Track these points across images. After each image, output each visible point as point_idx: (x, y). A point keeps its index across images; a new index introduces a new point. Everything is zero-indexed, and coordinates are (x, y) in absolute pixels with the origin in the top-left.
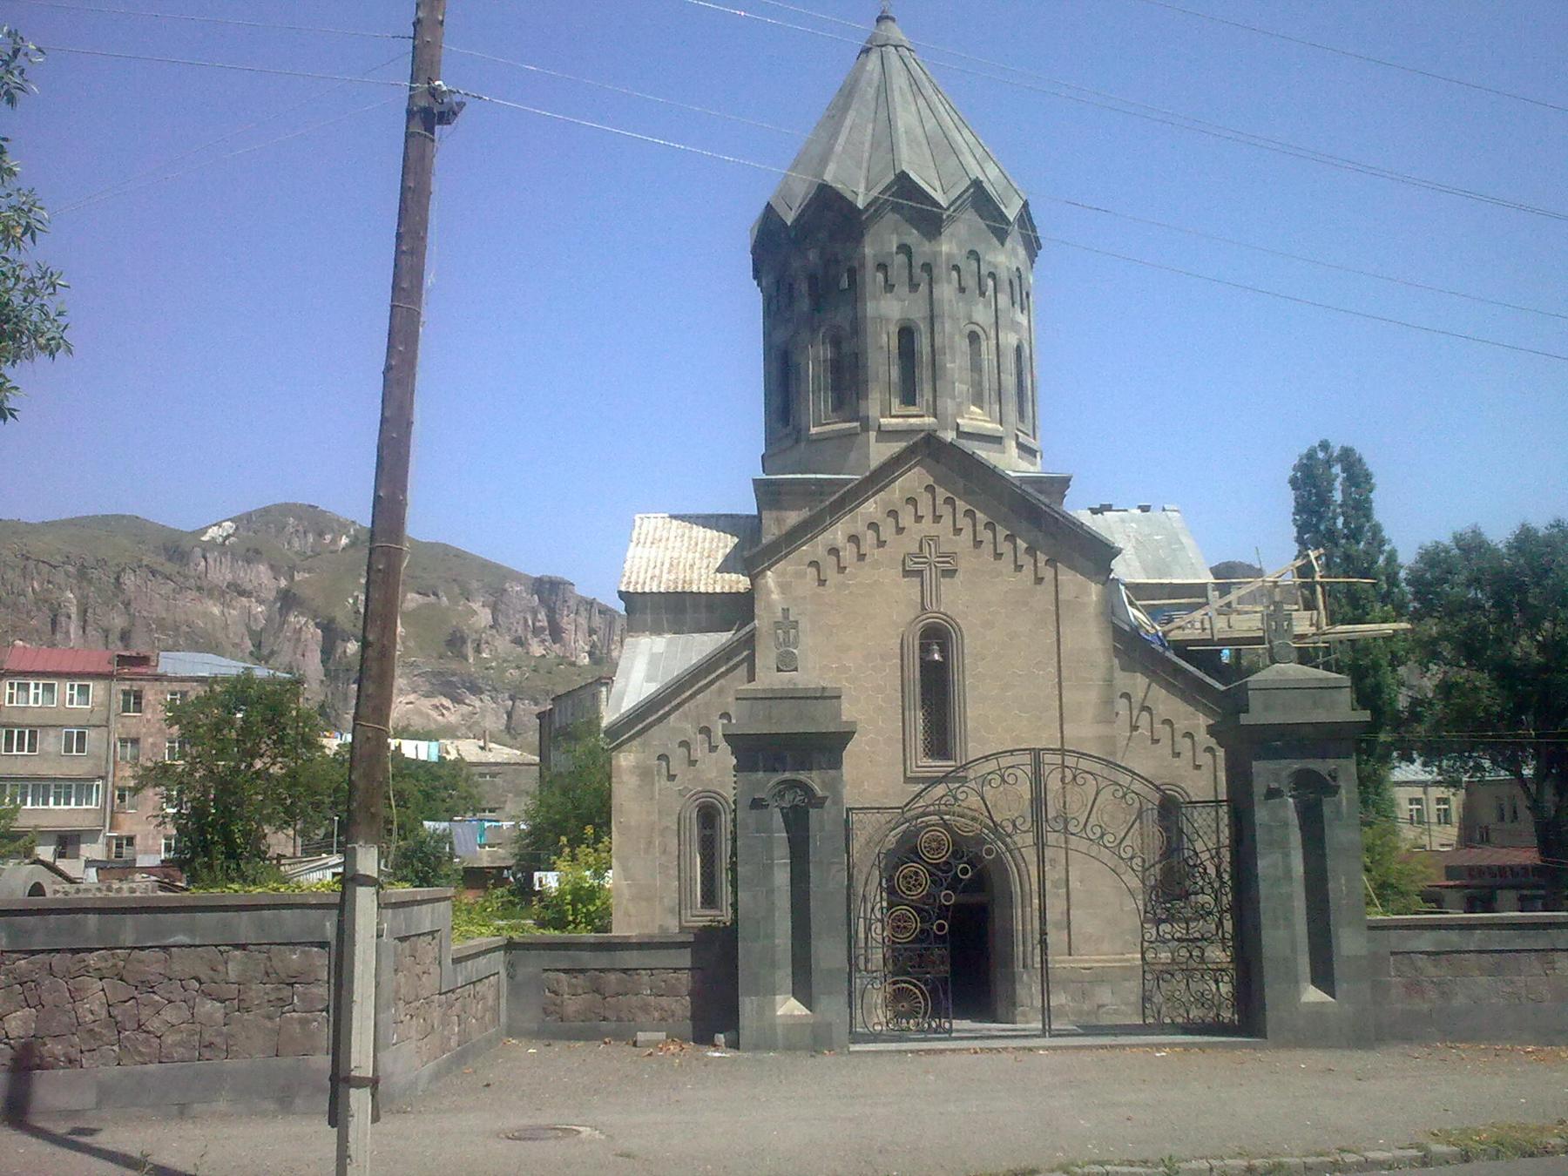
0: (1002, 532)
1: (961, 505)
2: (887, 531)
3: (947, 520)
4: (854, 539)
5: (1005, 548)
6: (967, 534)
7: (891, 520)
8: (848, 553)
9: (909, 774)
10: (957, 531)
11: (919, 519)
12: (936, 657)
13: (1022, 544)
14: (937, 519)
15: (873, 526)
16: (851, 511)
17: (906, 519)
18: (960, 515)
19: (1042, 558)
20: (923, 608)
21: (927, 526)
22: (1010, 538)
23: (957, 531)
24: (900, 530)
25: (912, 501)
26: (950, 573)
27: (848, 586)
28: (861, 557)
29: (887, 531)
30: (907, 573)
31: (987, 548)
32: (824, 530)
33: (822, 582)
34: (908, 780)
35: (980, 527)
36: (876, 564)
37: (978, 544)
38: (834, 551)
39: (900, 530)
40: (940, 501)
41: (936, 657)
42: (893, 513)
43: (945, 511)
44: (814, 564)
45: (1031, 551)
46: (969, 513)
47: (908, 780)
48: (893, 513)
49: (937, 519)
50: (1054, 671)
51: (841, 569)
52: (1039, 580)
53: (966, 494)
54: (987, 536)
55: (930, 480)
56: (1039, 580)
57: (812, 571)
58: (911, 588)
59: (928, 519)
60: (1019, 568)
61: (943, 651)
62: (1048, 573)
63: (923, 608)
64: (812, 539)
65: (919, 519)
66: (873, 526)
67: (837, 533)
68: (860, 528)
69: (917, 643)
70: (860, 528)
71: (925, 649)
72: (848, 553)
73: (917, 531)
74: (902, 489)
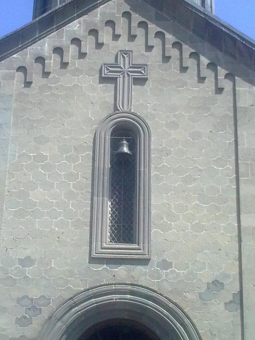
0: (187, 50)
1: (153, 28)
2: (88, 45)
3: (140, 41)
4: (58, 50)
5: (190, 63)
6: (157, 51)
7: (92, 38)
8: (53, 62)
9: (94, 255)
10: (149, 48)
11: (116, 37)
12: (126, 149)
13: (204, 61)
14: (132, 38)
15: (76, 41)
16: (58, 28)
17: (105, 36)
18: (151, 35)
19: (222, 72)
20: (116, 109)
21: (123, 43)
22: (195, 55)
23: (149, 48)
24: (99, 45)
25: (110, 23)
26: (141, 81)
27: (50, 88)
28: (64, 65)
29: (88, 45)
30: (103, 80)
31: (174, 63)
32: (34, 42)
33: (28, 84)
34: (93, 260)
35: (168, 46)
36: (76, 72)
37: (166, 59)
38: (40, 60)
39: (99, 45)
40: (134, 24)
41: (126, 149)
42: (94, 32)
43: (140, 32)
44: (22, 69)
45: (212, 66)
46: (159, 35)
47: (93, 260)
48: (94, 32)
49: (132, 38)
50: (231, 167)
51: (46, 74)
52: (219, 90)
53: (158, 19)
54: (174, 53)
55: (127, 8)
56: (219, 90)
57: (21, 74)
58: (106, 93)
59: (124, 38)
60: (201, 80)
61: (132, 146)
62: (227, 85)
63: (116, 109)
64: (22, 49)
65: (116, 37)
66: (76, 41)
67: (45, 46)
68: (65, 41)
69: (108, 137)
70: (65, 41)
71: (115, 144)
72: (53, 62)
73: (112, 47)
74: (102, 14)
